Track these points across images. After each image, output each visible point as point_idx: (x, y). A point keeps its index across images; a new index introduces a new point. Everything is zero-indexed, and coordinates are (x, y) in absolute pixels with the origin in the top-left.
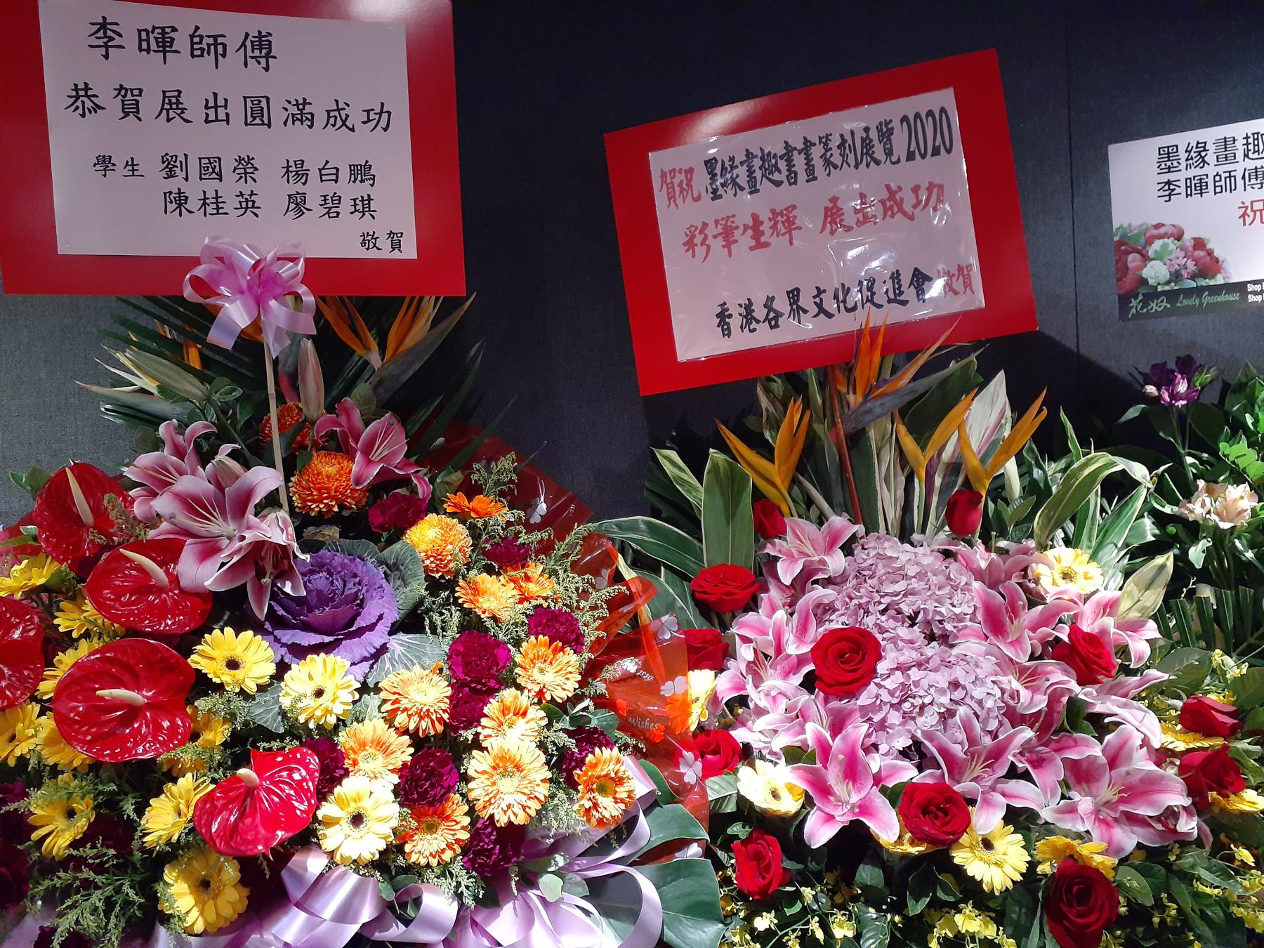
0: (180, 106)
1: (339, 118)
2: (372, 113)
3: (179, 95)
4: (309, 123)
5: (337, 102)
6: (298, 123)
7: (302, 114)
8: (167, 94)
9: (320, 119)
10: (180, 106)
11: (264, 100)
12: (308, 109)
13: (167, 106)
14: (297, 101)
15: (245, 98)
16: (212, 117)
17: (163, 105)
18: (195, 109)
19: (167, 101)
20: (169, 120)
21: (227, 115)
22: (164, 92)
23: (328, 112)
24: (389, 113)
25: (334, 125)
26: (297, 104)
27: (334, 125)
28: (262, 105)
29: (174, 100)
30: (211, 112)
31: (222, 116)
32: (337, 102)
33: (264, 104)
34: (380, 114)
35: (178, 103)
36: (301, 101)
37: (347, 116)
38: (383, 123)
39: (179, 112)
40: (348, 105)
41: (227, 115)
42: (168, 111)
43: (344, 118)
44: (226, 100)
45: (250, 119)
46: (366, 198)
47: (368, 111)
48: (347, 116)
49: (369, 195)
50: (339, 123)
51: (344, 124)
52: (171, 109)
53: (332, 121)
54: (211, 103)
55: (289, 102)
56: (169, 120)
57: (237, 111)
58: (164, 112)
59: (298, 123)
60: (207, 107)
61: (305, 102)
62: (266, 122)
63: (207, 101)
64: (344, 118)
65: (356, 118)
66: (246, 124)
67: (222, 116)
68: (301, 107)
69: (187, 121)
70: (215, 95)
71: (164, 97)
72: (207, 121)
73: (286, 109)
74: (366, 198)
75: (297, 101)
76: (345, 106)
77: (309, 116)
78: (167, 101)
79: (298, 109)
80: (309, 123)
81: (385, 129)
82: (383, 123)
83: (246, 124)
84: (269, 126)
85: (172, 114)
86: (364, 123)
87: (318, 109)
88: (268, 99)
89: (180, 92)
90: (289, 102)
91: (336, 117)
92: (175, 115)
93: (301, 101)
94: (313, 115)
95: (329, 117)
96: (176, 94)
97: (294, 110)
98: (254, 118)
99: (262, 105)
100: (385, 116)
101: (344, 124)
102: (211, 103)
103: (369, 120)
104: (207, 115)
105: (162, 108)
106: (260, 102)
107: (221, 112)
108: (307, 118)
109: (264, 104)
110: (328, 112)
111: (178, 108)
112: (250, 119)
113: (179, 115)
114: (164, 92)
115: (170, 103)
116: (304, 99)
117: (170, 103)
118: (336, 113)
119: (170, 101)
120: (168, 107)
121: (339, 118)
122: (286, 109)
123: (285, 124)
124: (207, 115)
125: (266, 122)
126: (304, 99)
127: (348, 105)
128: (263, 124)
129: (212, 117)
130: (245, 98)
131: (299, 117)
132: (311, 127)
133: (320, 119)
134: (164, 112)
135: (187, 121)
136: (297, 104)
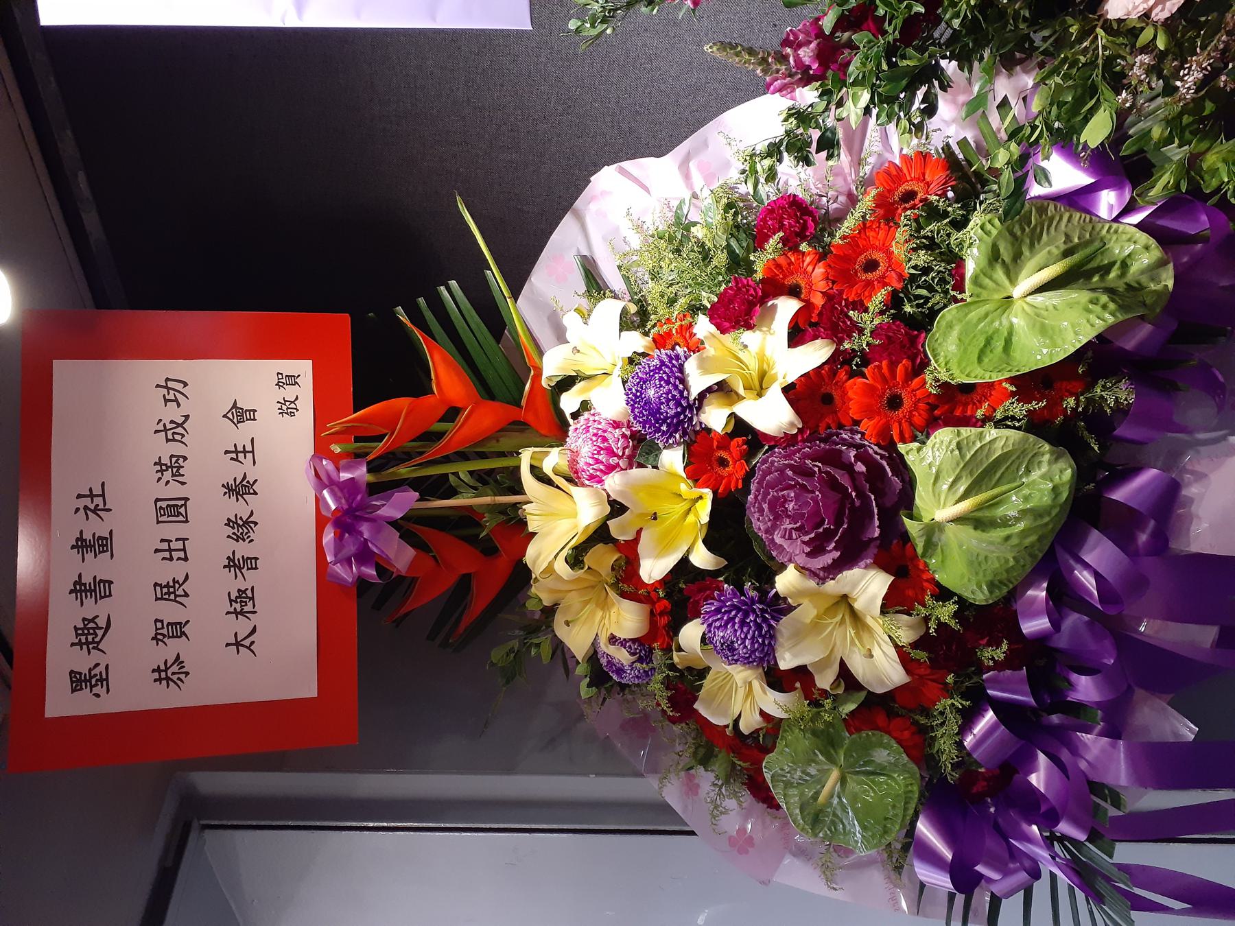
0: (171, 584)
2: (167, 397)
3: (160, 585)
4: (181, 460)
5: (156, 432)
6: (181, 471)
7: (172, 467)
8: (159, 596)
9: (177, 449)
10: (171, 584)
11: (159, 504)
12: (166, 460)
13: (172, 597)
14: (157, 472)
15: (158, 522)
16: (181, 554)
18: (175, 570)
19: (167, 597)
20: (186, 595)
21: (177, 540)
22: (157, 599)
23: (168, 440)
24: (167, 380)
26: (162, 471)
28: (164, 506)
29: (165, 590)
31: (180, 545)
32: (156, 432)
33: (163, 504)
34: (166, 387)
35: (167, 586)
36: (158, 467)
37: (172, 422)
38: (179, 386)
39: (177, 586)
40: (160, 421)
41: (177, 540)
42: (176, 596)
43: (174, 425)
44: (162, 541)
45: (181, 518)
47: (166, 401)
48: (172, 422)
50: (180, 430)
52: (174, 592)
53: (178, 437)
54: (167, 555)
55: (159, 479)
56: (186, 595)
57: (173, 531)
58: (177, 599)
59: (181, 471)
60: (171, 559)
61: (159, 463)
62: (183, 502)
63: (164, 559)
64: (174, 425)
65: (173, 413)
66: (187, 521)
67: (180, 545)
68: (164, 468)
69: (187, 578)
70: (157, 551)
71: (162, 599)
72: (186, 559)
73: (168, 482)
75: (157, 472)
76: (162, 423)
77: (174, 460)
78: (167, 597)
79: (167, 470)
80: (181, 460)
81: (185, 384)
82: (179, 386)
83: (187, 521)
84: (187, 499)
85: (180, 592)
86: (179, 405)
87: (167, 451)
88: (157, 500)
89: (156, 585)
90: (159, 479)
91: (174, 433)
93: (158, 467)
94: (172, 456)
95: (174, 440)
96: (158, 588)
97: (168, 475)
98: (180, 514)
99: (164, 506)
100: (170, 384)
101: (179, 425)
102: (167, 555)
103: (176, 400)
104: (179, 559)
105: (175, 601)
106: (161, 508)
107: (174, 545)
108: (176, 462)
109: (163, 504)
110: (168, 440)
111: (174, 587)
112: (181, 518)
113: (180, 586)
114: (157, 599)
115: (169, 593)
116: (155, 464)
117: (169, 593)
118: (169, 433)
119: (166, 594)
120: (172, 597)
122: (168, 482)
123: (183, 483)
124: (179, 559)
125: (183, 502)
126: (155, 464)
127: (160, 421)
128: (185, 505)
129: (181, 554)
130: (158, 522)
131: (175, 470)
132: (185, 459)
133: (177, 449)
134: (177, 599)
135: (187, 578)
136: (162, 471)
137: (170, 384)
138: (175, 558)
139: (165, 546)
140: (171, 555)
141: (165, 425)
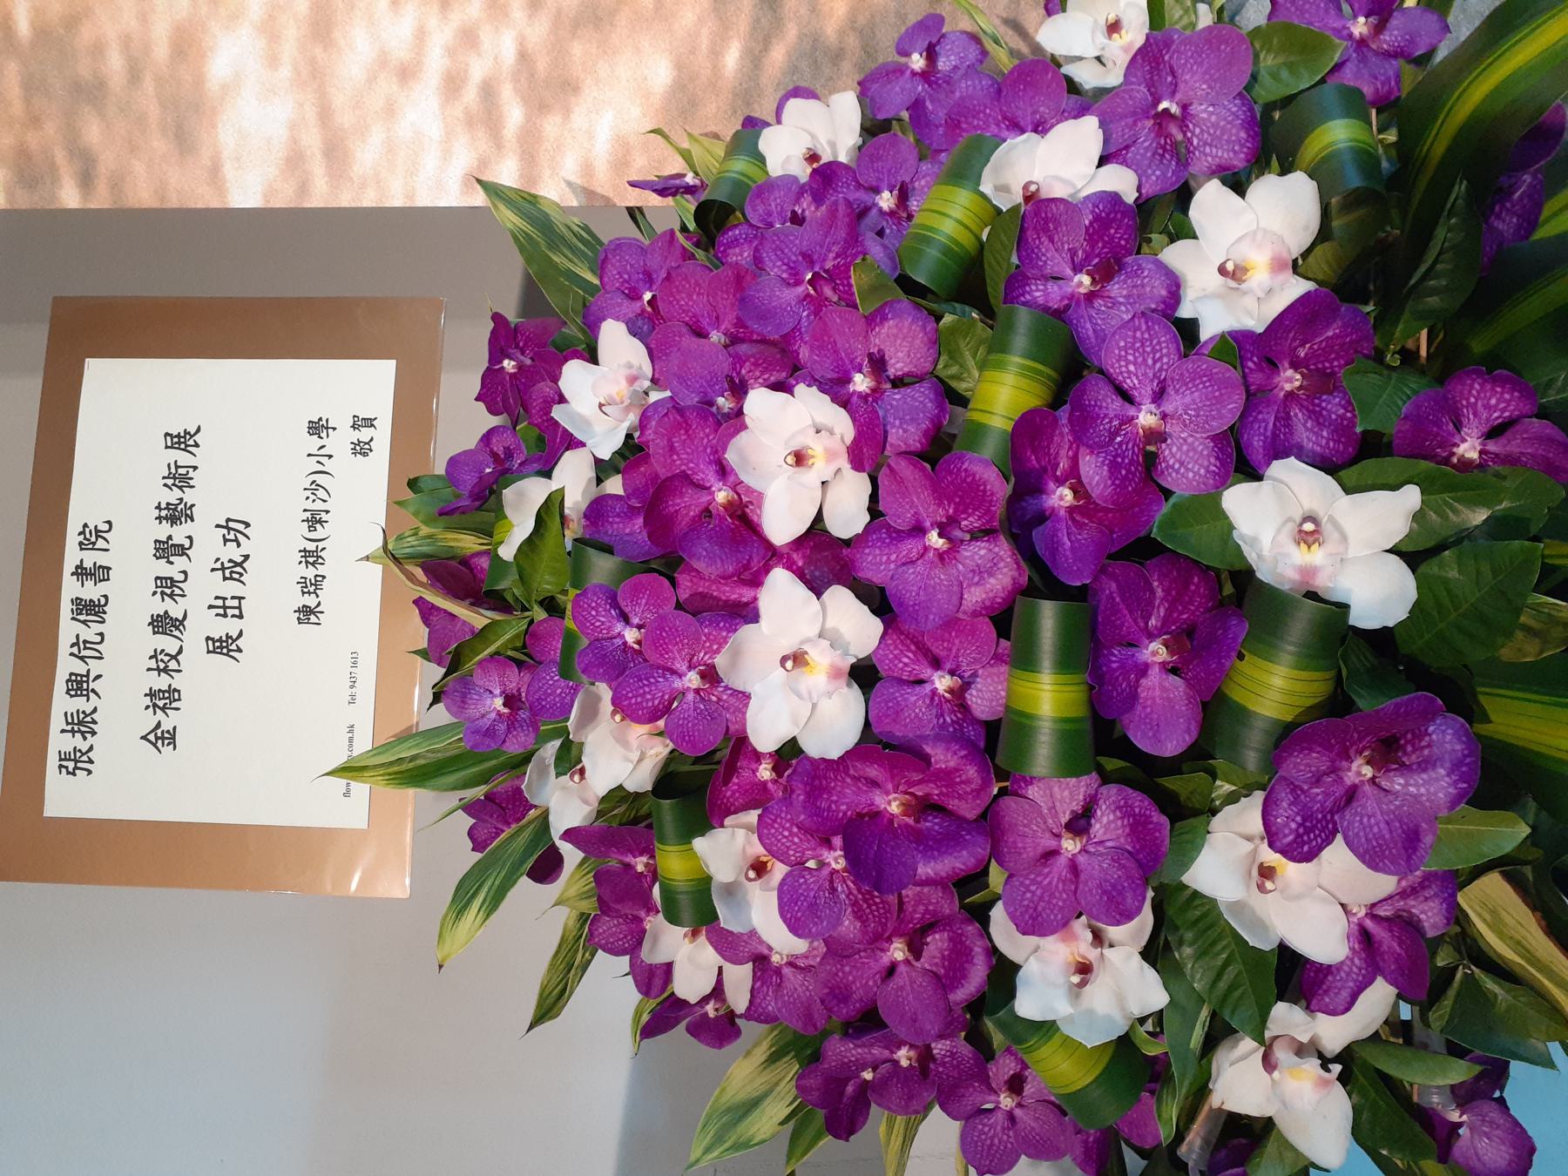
0: (224, 638)
1: (234, 569)
2: (227, 537)
3: (212, 639)
10: (224, 638)
13: (225, 651)
16: (236, 612)
17: (224, 654)
18: (230, 626)
21: (233, 598)
25: (241, 575)
27: (241, 575)
29: (217, 644)
30: (230, 612)
31: (235, 603)
34: (229, 529)
35: (220, 640)
39: (230, 641)
41: (233, 598)
44: (217, 598)
46: (303, 554)
47: (226, 541)
49: (300, 551)
50: (238, 569)
51: (240, 565)
54: (221, 611)
56: (239, 650)
58: (231, 653)
60: (225, 615)
63: (217, 615)
67: (235, 603)
70: (210, 607)
72: (241, 617)
74: (303, 554)
85: (234, 647)
89: (208, 638)
92: (234, 645)
102: (221, 611)
103: (236, 540)
104: (233, 616)
105: (227, 655)
107: (228, 603)
111: (227, 641)
114: (209, 652)
115: (222, 648)
119: (218, 648)
121: (234, 569)
124: (233, 616)
129: (236, 612)
134: (231, 653)
137: (231, 524)
138: (230, 615)
139: (220, 603)
140: (225, 612)
141: (222, 563)
